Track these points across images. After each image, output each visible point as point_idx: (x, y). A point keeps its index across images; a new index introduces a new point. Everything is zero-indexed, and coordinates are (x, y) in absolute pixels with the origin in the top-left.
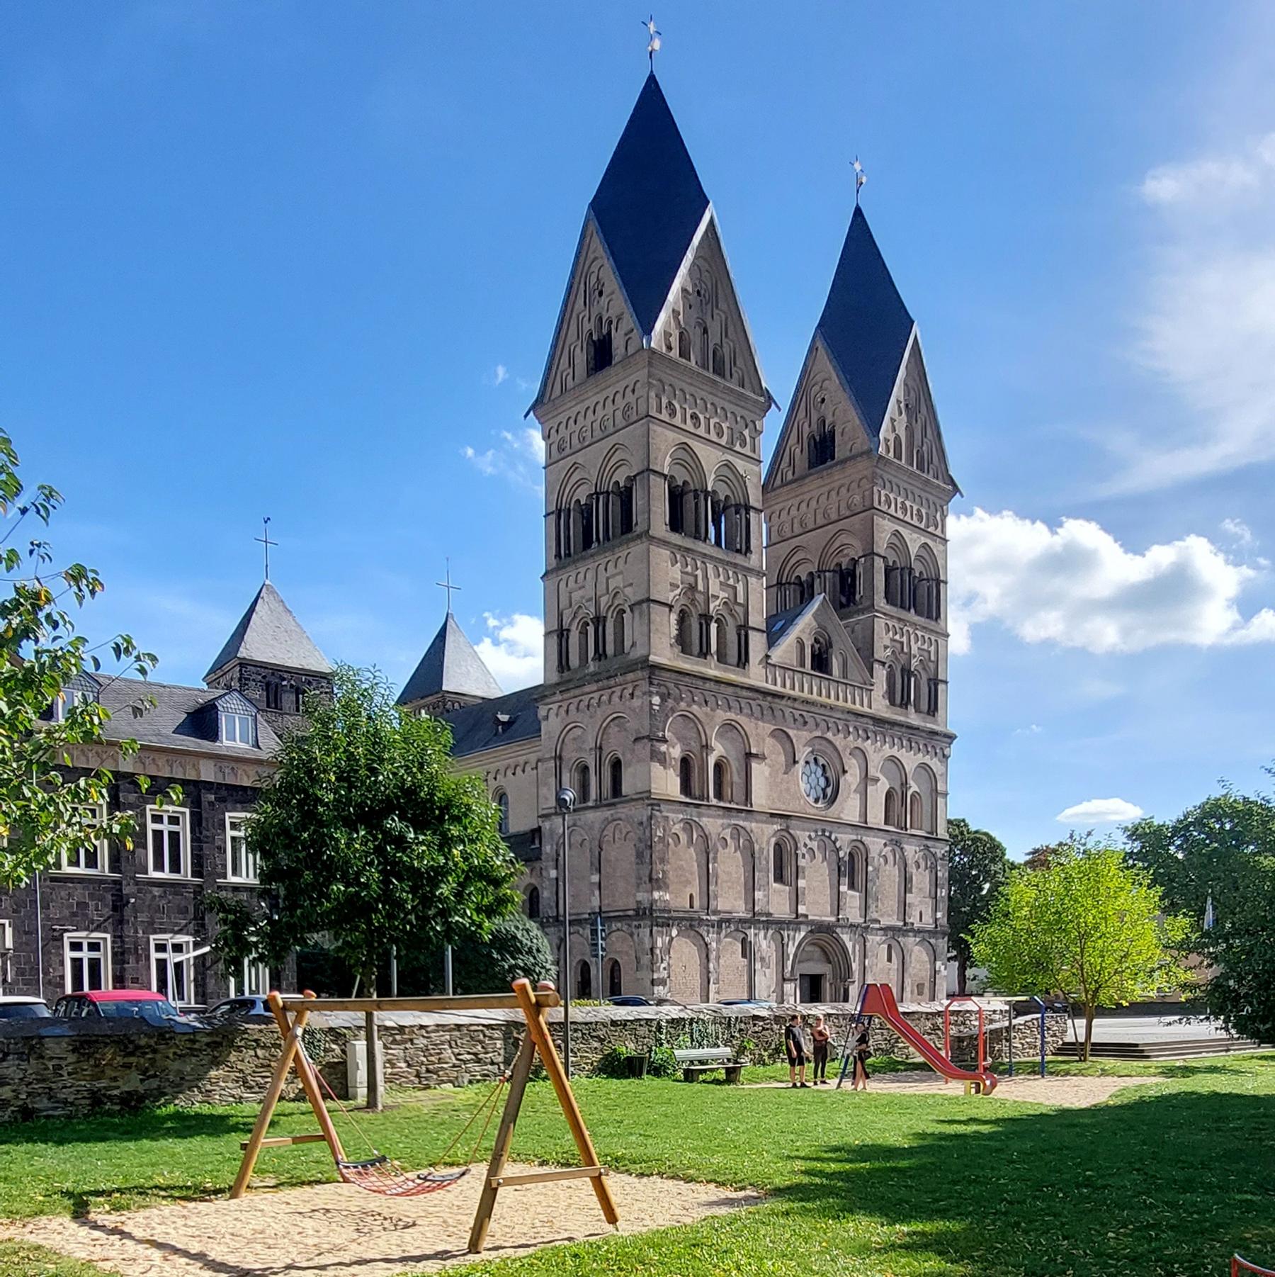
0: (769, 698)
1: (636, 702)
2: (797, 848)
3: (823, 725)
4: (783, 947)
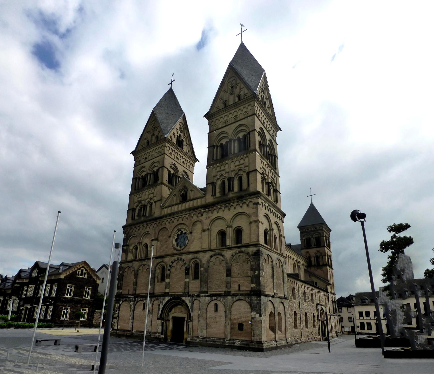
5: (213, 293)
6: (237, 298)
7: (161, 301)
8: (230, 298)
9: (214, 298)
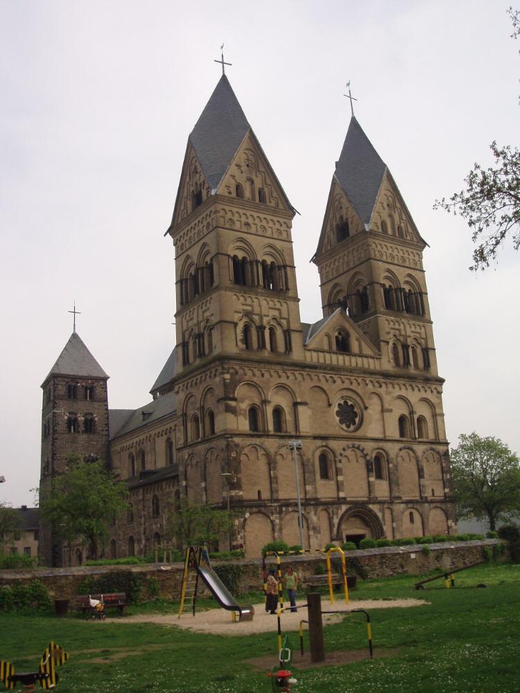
0: (308, 370)
1: (217, 379)
2: (335, 456)
3: (347, 381)
4: (330, 519)
5: (411, 498)
6: (434, 505)
7: (335, 511)
8: (426, 505)
9: (410, 505)
